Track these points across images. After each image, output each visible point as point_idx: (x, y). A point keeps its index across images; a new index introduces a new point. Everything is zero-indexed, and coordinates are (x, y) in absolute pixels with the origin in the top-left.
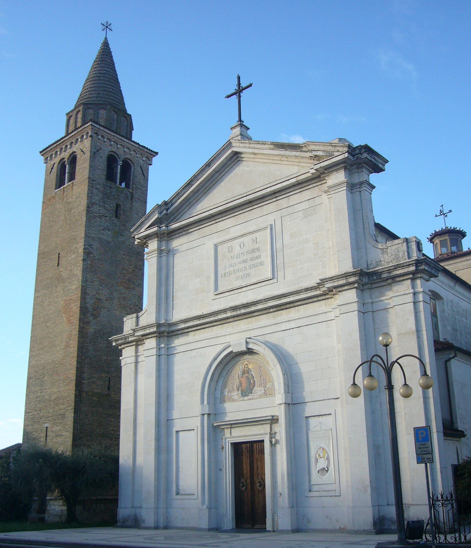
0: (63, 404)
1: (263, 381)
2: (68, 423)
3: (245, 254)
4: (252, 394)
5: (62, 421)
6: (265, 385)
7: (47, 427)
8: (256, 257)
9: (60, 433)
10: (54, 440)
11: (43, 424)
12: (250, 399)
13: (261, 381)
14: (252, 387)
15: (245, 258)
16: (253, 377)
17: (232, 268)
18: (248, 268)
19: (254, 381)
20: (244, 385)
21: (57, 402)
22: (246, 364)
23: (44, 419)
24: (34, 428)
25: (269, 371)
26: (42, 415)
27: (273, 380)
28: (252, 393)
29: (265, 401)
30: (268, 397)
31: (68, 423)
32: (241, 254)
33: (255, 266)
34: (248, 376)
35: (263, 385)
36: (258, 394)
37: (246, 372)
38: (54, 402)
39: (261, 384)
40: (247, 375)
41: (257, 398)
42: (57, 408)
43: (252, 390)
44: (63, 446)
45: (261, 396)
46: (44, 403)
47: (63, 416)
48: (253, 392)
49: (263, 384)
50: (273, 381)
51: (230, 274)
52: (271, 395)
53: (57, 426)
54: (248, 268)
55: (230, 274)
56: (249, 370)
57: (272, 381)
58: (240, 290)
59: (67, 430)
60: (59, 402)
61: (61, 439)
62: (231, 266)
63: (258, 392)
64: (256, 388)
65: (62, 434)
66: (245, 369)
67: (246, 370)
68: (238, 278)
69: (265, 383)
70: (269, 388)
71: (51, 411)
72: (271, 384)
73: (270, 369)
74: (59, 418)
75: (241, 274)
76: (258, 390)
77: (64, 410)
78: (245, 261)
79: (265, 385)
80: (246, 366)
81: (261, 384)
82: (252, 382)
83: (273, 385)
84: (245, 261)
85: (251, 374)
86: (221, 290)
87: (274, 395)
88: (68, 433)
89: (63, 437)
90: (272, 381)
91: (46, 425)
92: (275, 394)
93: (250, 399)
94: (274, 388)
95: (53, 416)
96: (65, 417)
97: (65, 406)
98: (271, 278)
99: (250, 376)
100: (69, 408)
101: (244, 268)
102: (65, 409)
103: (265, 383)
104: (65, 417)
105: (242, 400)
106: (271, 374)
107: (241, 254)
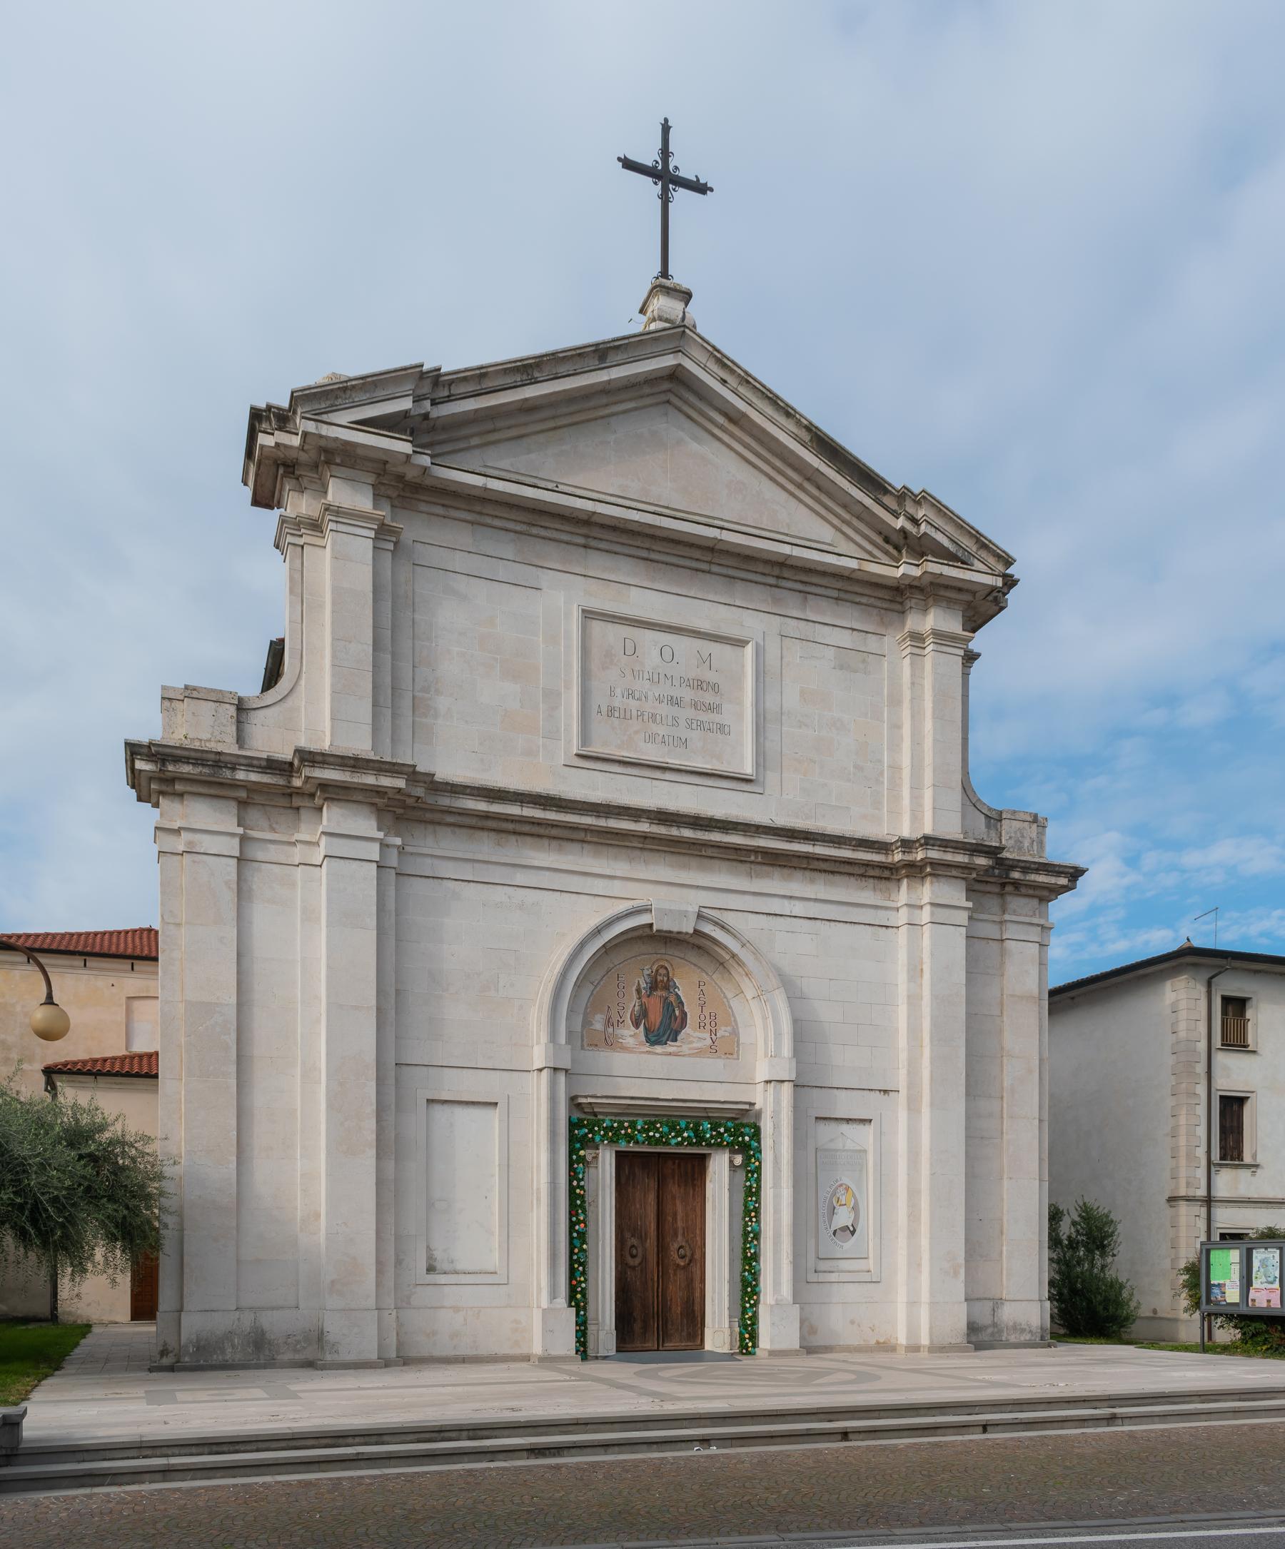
1: (708, 1017)
3: (676, 682)
4: (677, 1044)
6: (713, 1030)
8: (707, 705)
12: (670, 1054)
13: (702, 1017)
14: (675, 1026)
15: (676, 693)
16: (682, 1003)
17: (633, 704)
18: (682, 723)
19: (684, 1014)
20: (656, 1016)
22: (662, 967)
25: (726, 997)
27: (735, 1021)
28: (676, 1040)
29: (713, 1067)
30: (720, 1057)
32: (662, 676)
33: (701, 725)
34: (667, 998)
35: (708, 1027)
36: (695, 1045)
37: (660, 984)
39: (702, 1024)
40: (664, 994)
41: (689, 1055)
43: (677, 1033)
45: (699, 1053)
48: (679, 1038)
49: (708, 1025)
50: (737, 1024)
51: (625, 716)
52: (727, 1056)
54: (682, 723)
55: (625, 716)
56: (671, 983)
57: (733, 1024)
58: (658, 774)
62: (631, 694)
63: (691, 1042)
64: (687, 1030)
66: (659, 978)
67: (662, 981)
68: (652, 738)
69: (713, 1024)
70: (723, 1036)
72: (729, 1028)
73: (730, 995)
75: (661, 730)
76: (693, 1036)
78: (675, 702)
79: (713, 1030)
80: (662, 971)
81: (702, 1024)
82: (677, 1013)
83: (735, 1033)
84: (675, 702)
85: (677, 994)
86: (597, 749)
87: (735, 1056)
90: (733, 1024)
92: (738, 1055)
93: (670, 1054)
94: (738, 1041)
98: (753, 778)
99: (672, 999)
101: (670, 719)
103: (713, 1024)
105: (648, 1052)
106: (730, 1007)
107: (662, 676)
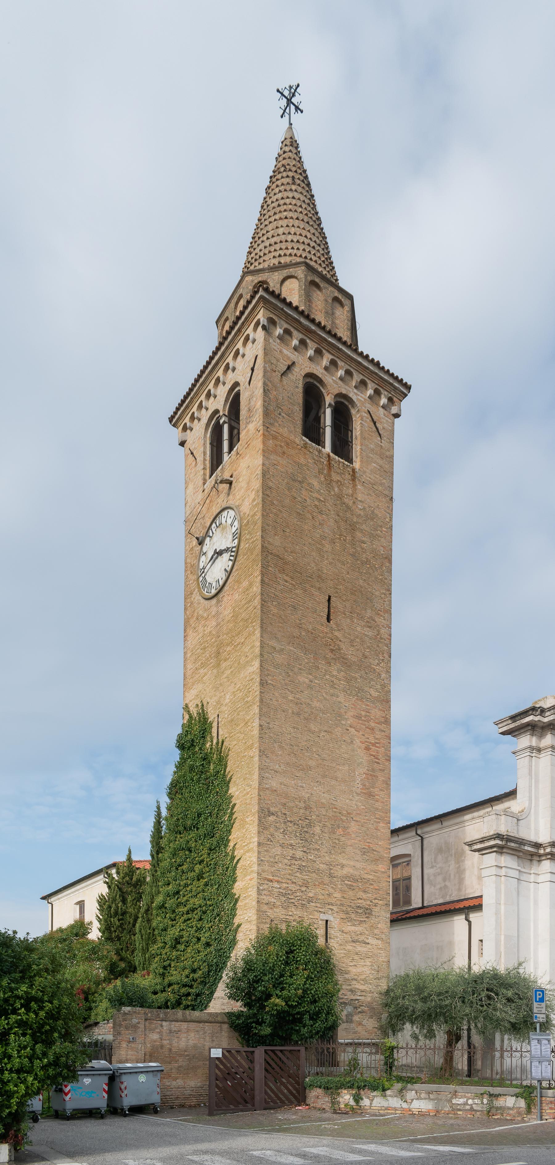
0: (365, 892)
2: (379, 926)
5: (366, 919)
7: (327, 921)
9: (362, 938)
10: (349, 947)
11: (316, 913)
21: (349, 883)
23: (319, 905)
24: (290, 913)
26: (311, 895)
31: (379, 926)
38: (344, 881)
42: (351, 893)
44: (370, 960)
46: (314, 875)
47: (368, 912)
53: (354, 925)
59: (377, 937)
60: (354, 884)
61: (365, 949)
65: (367, 941)
71: (335, 895)
74: (357, 912)
77: (368, 903)
88: (380, 942)
89: (369, 946)
91: (325, 917)
95: (342, 905)
96: (370, 914)
97: (370, 895)
100: (380, 902)
102: (371, 902)
104: (370, 914)
